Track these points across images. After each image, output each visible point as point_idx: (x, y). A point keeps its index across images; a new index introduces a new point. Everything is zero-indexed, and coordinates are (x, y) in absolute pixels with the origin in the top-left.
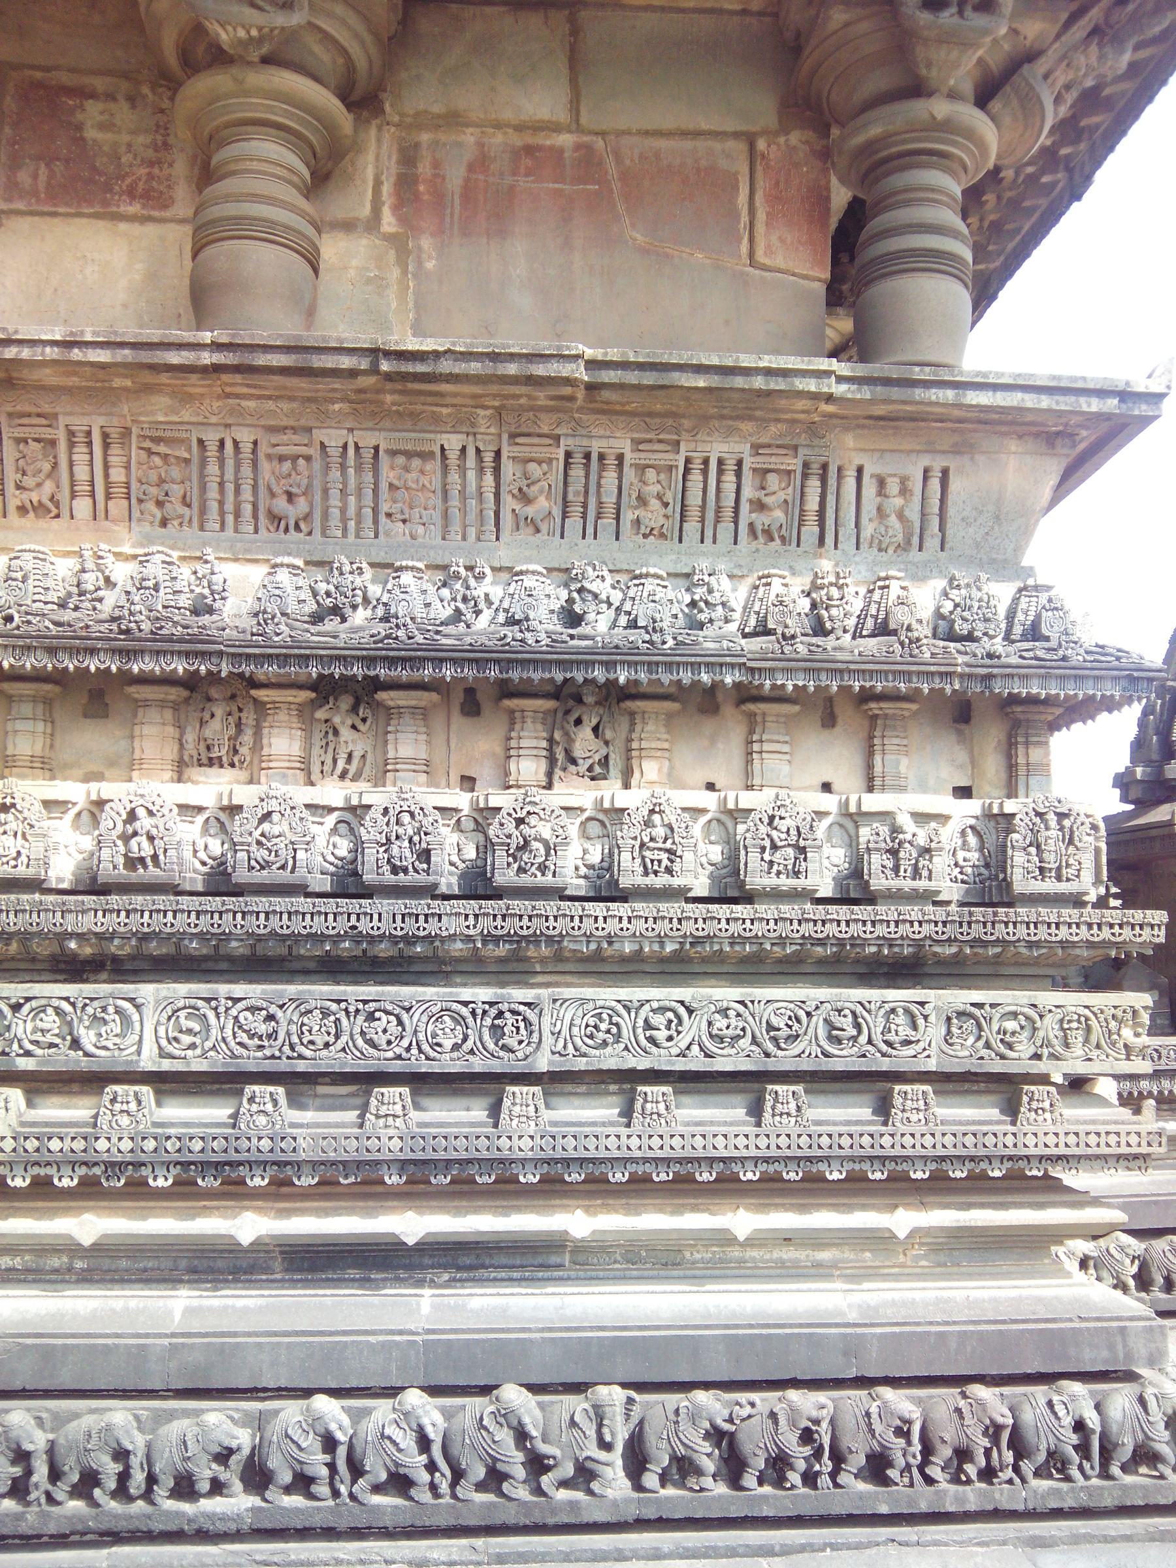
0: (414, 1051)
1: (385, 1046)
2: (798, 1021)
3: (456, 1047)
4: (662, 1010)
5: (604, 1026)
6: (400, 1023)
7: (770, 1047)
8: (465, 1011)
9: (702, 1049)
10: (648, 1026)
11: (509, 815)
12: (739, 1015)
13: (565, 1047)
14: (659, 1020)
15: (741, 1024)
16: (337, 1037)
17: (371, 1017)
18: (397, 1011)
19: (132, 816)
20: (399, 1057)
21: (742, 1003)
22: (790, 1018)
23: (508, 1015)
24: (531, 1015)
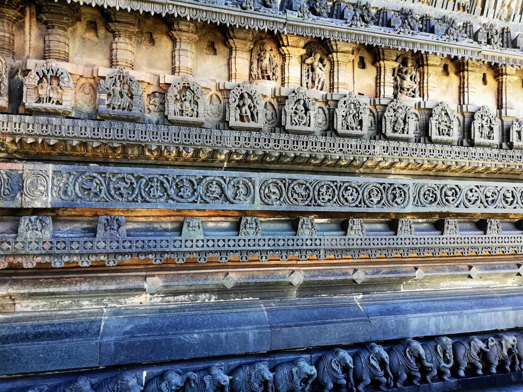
0: (363, 204)
1: (351, 202)
2: (495, 194)
3: (379, 202)
4: (451, 189)
5: (431, 195)
6: (357, 191)
7: (486, 204)
8: (381, 188)
9: (464, 205)
10: (446, 195)
11: (391, 107)
12: (476, 191)
13: (417, 203)
14: (450, 193)
15: (477, 195)
16: (333, 197)
17: (346, 189)
18: (356, 186)
19: (242, 97)
20: (357, 206)
21: (477, 187)
22: (493, 193)
23: (397, 189)
24: (406, 190)
